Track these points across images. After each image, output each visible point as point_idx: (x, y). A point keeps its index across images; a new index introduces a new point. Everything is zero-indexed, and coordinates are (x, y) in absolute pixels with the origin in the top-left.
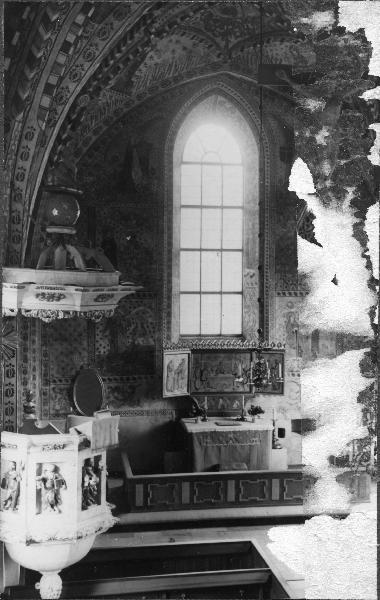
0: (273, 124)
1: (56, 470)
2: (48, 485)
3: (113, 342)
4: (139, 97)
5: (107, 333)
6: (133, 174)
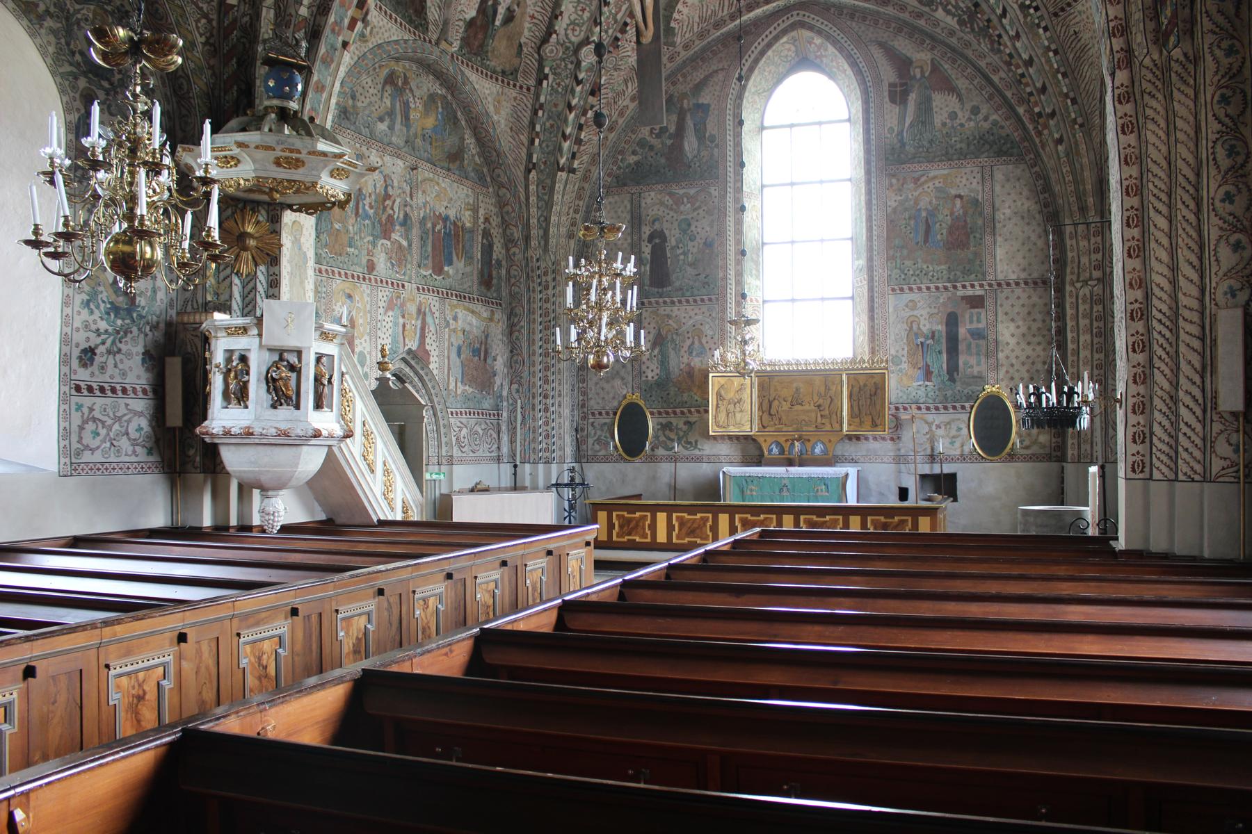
0: (877, 53)
1: (244, 359)
2: (232, 375)
3: (664, 362)
4: (686, 47)
5: (656, 352)
6: (686, 144)
